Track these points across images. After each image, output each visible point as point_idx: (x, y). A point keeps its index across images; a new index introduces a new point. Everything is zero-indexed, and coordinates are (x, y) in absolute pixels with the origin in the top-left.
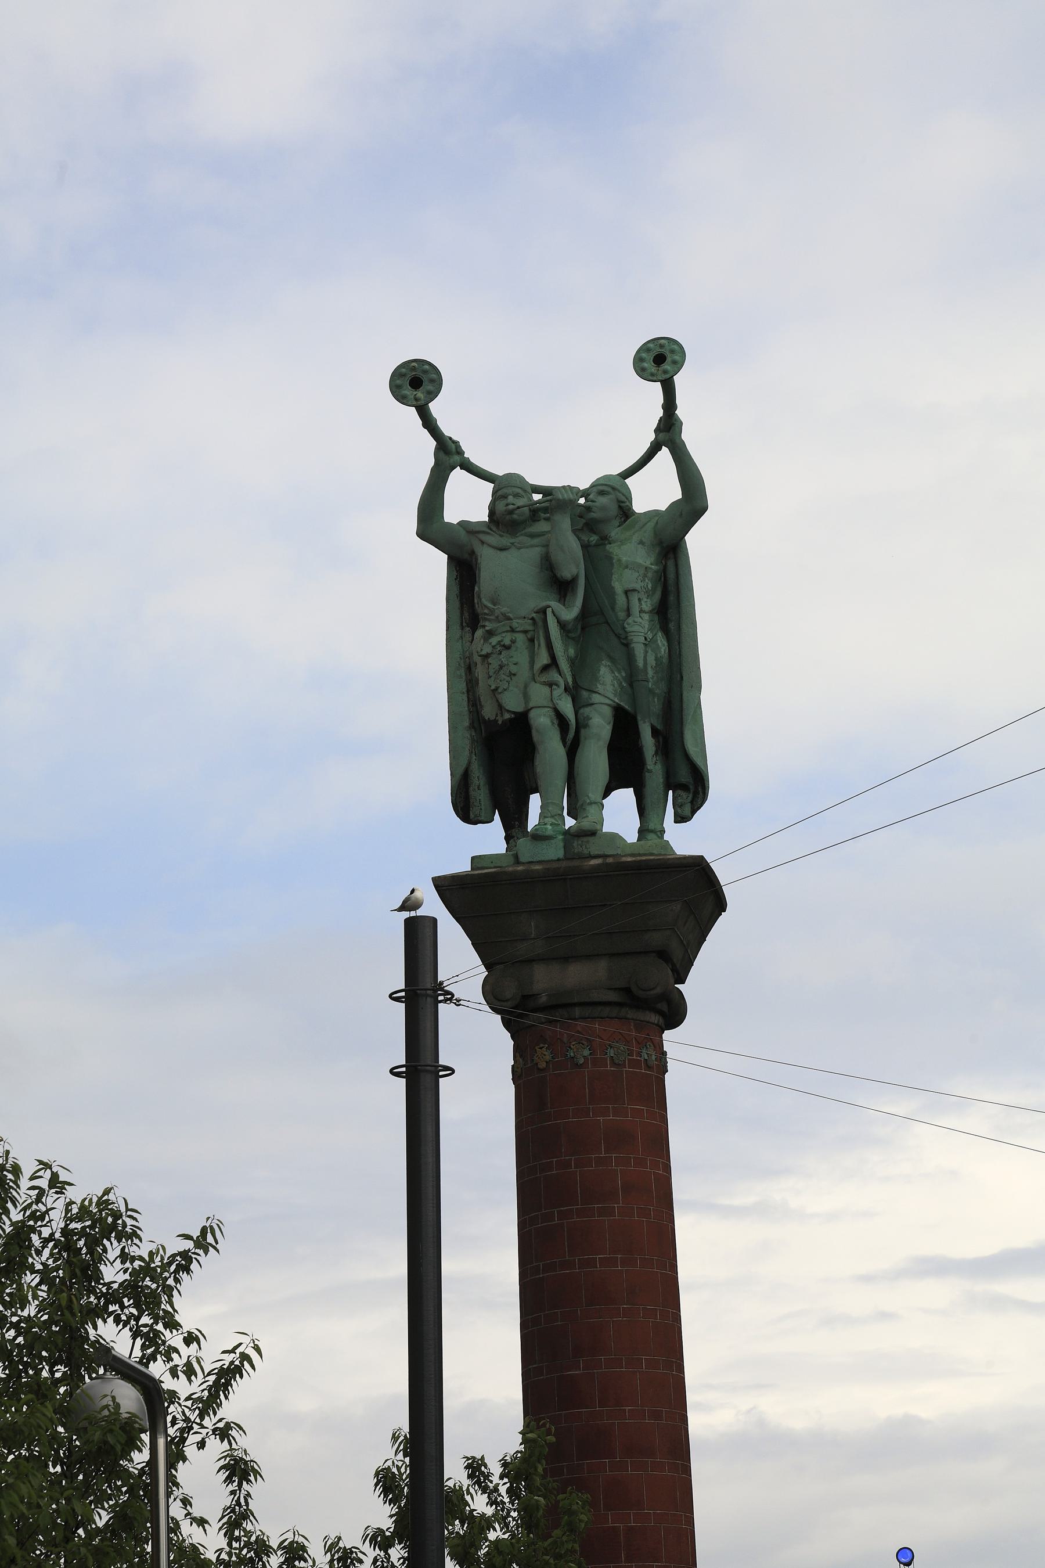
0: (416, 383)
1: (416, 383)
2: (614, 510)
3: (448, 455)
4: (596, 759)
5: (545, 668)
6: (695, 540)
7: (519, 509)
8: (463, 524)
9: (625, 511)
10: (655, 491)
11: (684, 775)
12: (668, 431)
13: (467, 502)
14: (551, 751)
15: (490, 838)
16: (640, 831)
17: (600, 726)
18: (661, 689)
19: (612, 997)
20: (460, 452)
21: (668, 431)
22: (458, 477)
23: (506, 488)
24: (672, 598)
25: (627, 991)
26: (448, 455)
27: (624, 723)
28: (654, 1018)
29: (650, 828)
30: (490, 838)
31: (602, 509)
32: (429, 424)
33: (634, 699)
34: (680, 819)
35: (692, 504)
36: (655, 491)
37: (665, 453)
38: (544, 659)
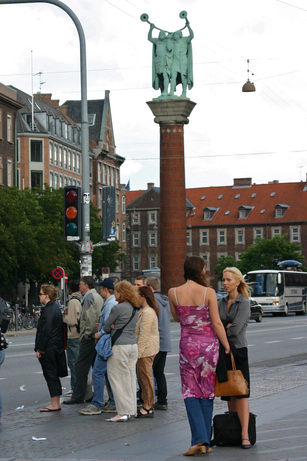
0: (144, 17)
1: (144, 18)
2: (179, 37)
3: (152, 26)
4: (174, 80)
5: (166, 66)
6: (193, 41)
7: (163, 38)
8: (155, 38)
9: (181, 37)
10: (186, 33)
11: (189, 83)
12: (187, 23)
13: (156, 34)
14: (166, 79)
15: (157, 94)
16: (183, 92)
17: (175, 76)
18: (186, 68)
19: (173, 122)
20: (154, 26)
21: (187, 23)
22: (154, 30)
23: (162, 32)
24: (189, 52)
25: (176, 121)
26: (152, 26)
27: (179, 75)
28: (181, 125)
29: (184, 92)
30: (157, 94)
31: (175, 37)
32: (148, 22)
33: (181, 71)
34: (189, 89)
35: (191, 36)
36: (186, 33)
37: (187, 27)
38: (166, 64)
